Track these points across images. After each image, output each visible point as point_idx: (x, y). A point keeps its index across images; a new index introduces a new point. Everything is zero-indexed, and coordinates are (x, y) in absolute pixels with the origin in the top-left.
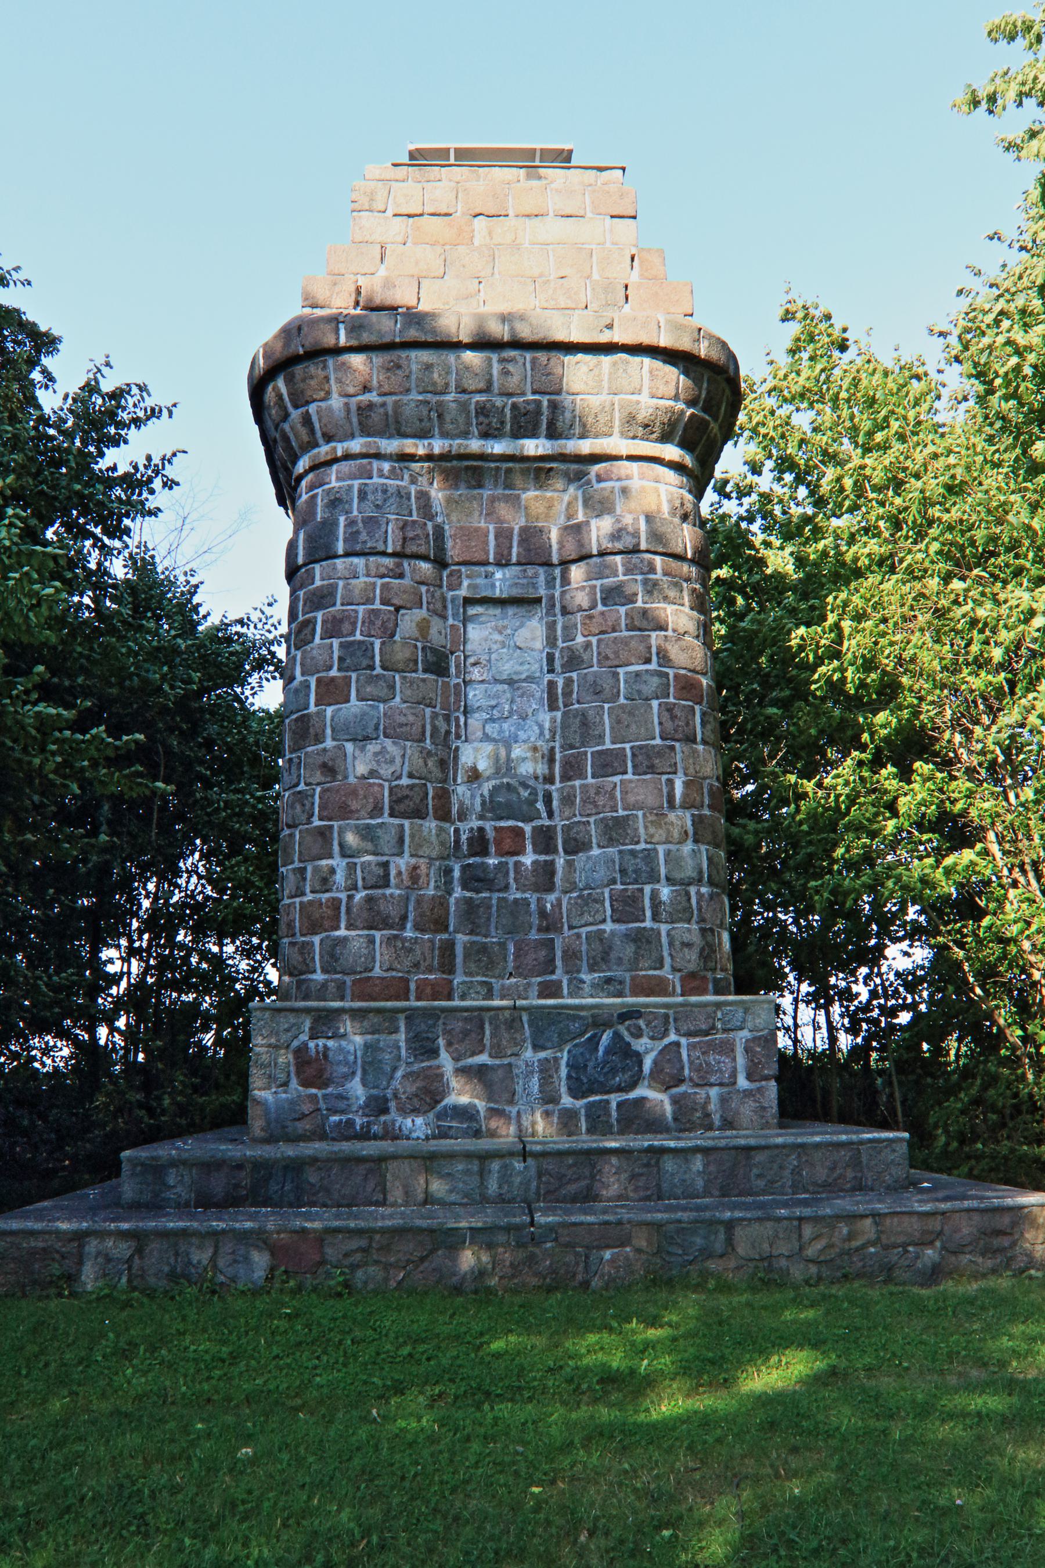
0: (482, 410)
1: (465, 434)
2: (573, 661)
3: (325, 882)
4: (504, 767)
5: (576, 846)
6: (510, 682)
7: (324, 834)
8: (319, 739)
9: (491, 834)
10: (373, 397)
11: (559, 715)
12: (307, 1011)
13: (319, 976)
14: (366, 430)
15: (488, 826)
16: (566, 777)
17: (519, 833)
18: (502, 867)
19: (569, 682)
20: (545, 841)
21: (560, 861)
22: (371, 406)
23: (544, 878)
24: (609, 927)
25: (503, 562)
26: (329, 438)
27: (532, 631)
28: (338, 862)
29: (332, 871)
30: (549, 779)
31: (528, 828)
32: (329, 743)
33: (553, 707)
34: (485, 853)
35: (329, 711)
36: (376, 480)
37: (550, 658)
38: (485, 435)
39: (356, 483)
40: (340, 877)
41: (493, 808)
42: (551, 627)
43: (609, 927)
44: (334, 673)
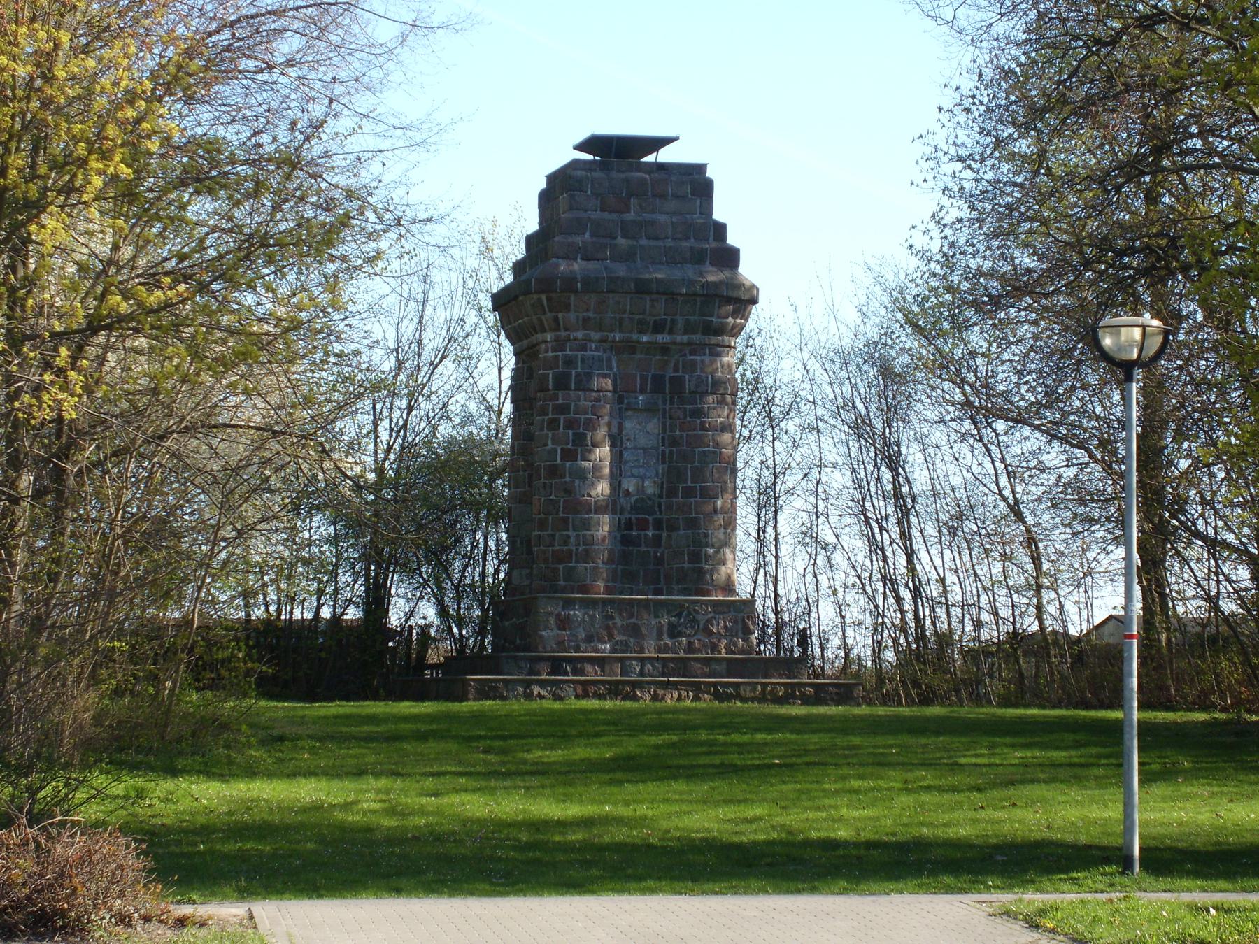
0: (641, 322)
1: (631, 332)
2: (674, 442)
3: (566, 541)
4: (641, 490)
5: (672, 528)
6: (644, 449)
7: (565, 520)
8: (563, 476)
9: (634, 520)
10: (591, 314)
11: (666, 466)
12: (561, 598)
13: (562, 583)
14: (585, 328)
15: (633, 517)
16: (668, 497)
17: (647, 520)
18: (639, 535)
19: (671, 452)
20: (658, 525)
21: (665, 534)
22: (589, 318)
23: (657, 541)
24: (686, 565)
25: (642, 391)
26: (566, 330)
27: (653, 426)
28: (571, 533)
29: (569, 537)
30: (661, 496)
31: (650, 519)
32: (567, 479)
33: (663, 463)
34: (631, 529)
35: (568, 464)
36: (589, 353)
37: (663, 439)
38: (640, 332)
39: (580, 354)
40: (572, 540)
41: (635, 509)
42: (664, 424)
43: (686, 565)
44: (570, 446)
